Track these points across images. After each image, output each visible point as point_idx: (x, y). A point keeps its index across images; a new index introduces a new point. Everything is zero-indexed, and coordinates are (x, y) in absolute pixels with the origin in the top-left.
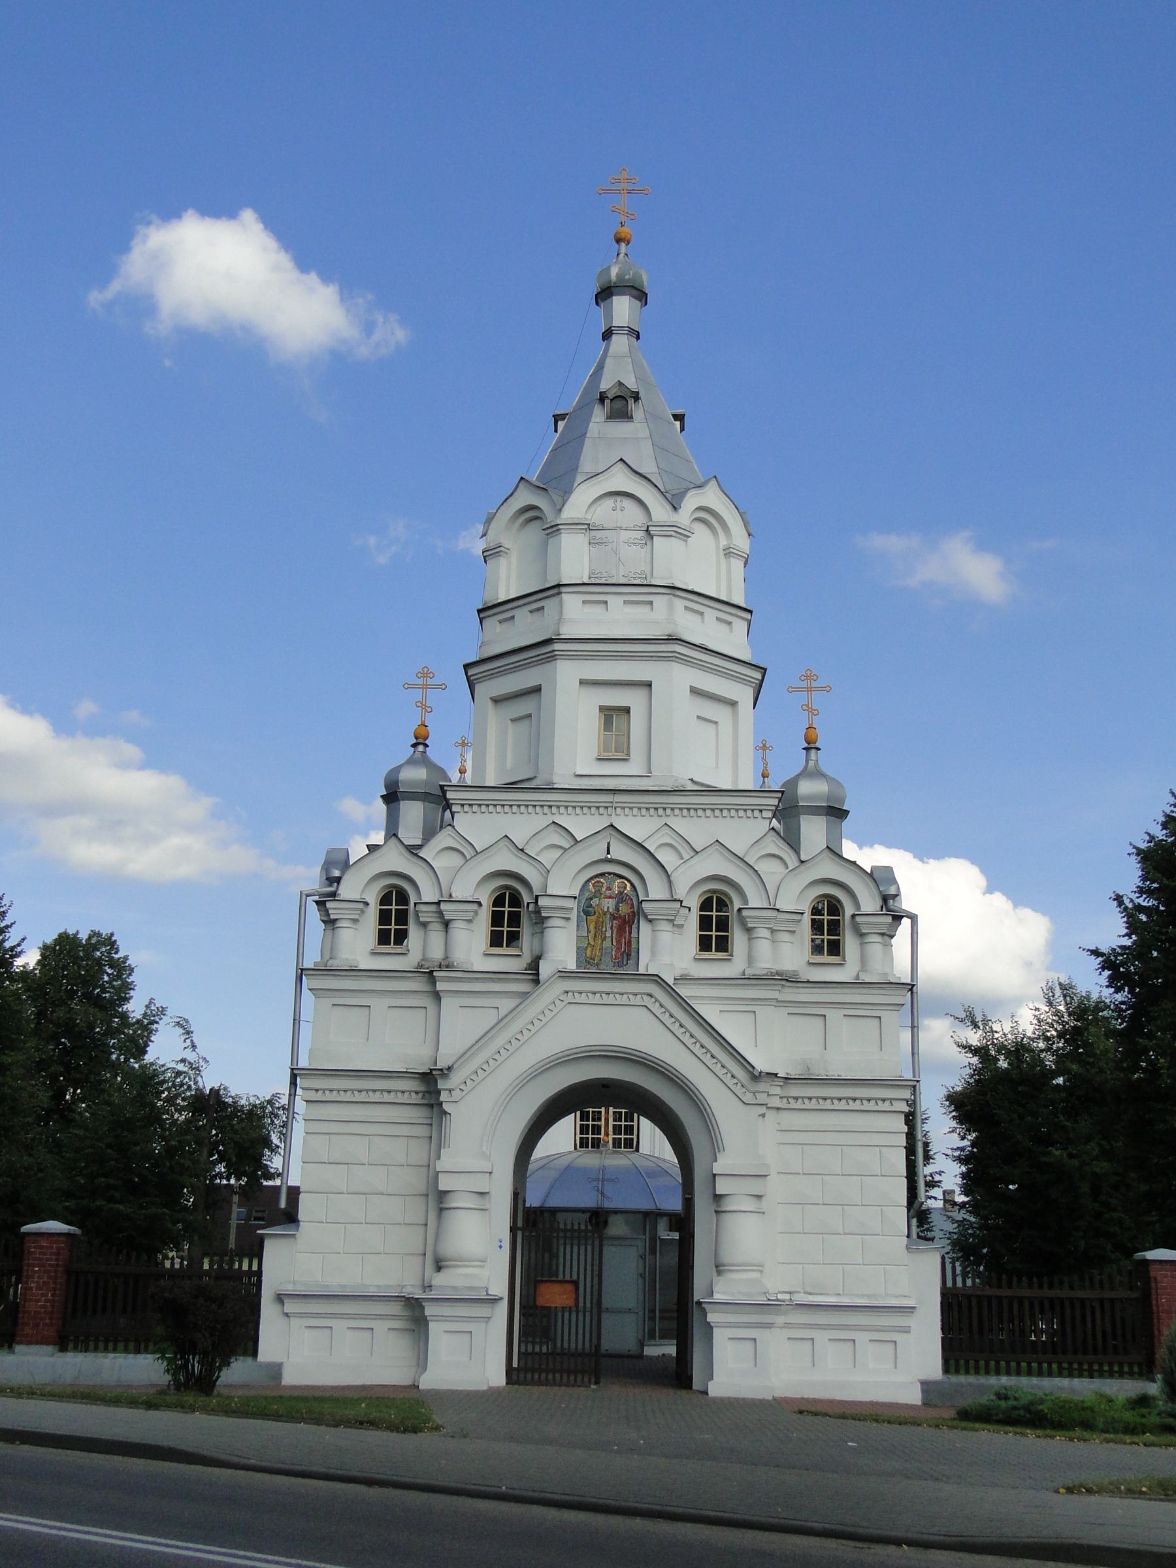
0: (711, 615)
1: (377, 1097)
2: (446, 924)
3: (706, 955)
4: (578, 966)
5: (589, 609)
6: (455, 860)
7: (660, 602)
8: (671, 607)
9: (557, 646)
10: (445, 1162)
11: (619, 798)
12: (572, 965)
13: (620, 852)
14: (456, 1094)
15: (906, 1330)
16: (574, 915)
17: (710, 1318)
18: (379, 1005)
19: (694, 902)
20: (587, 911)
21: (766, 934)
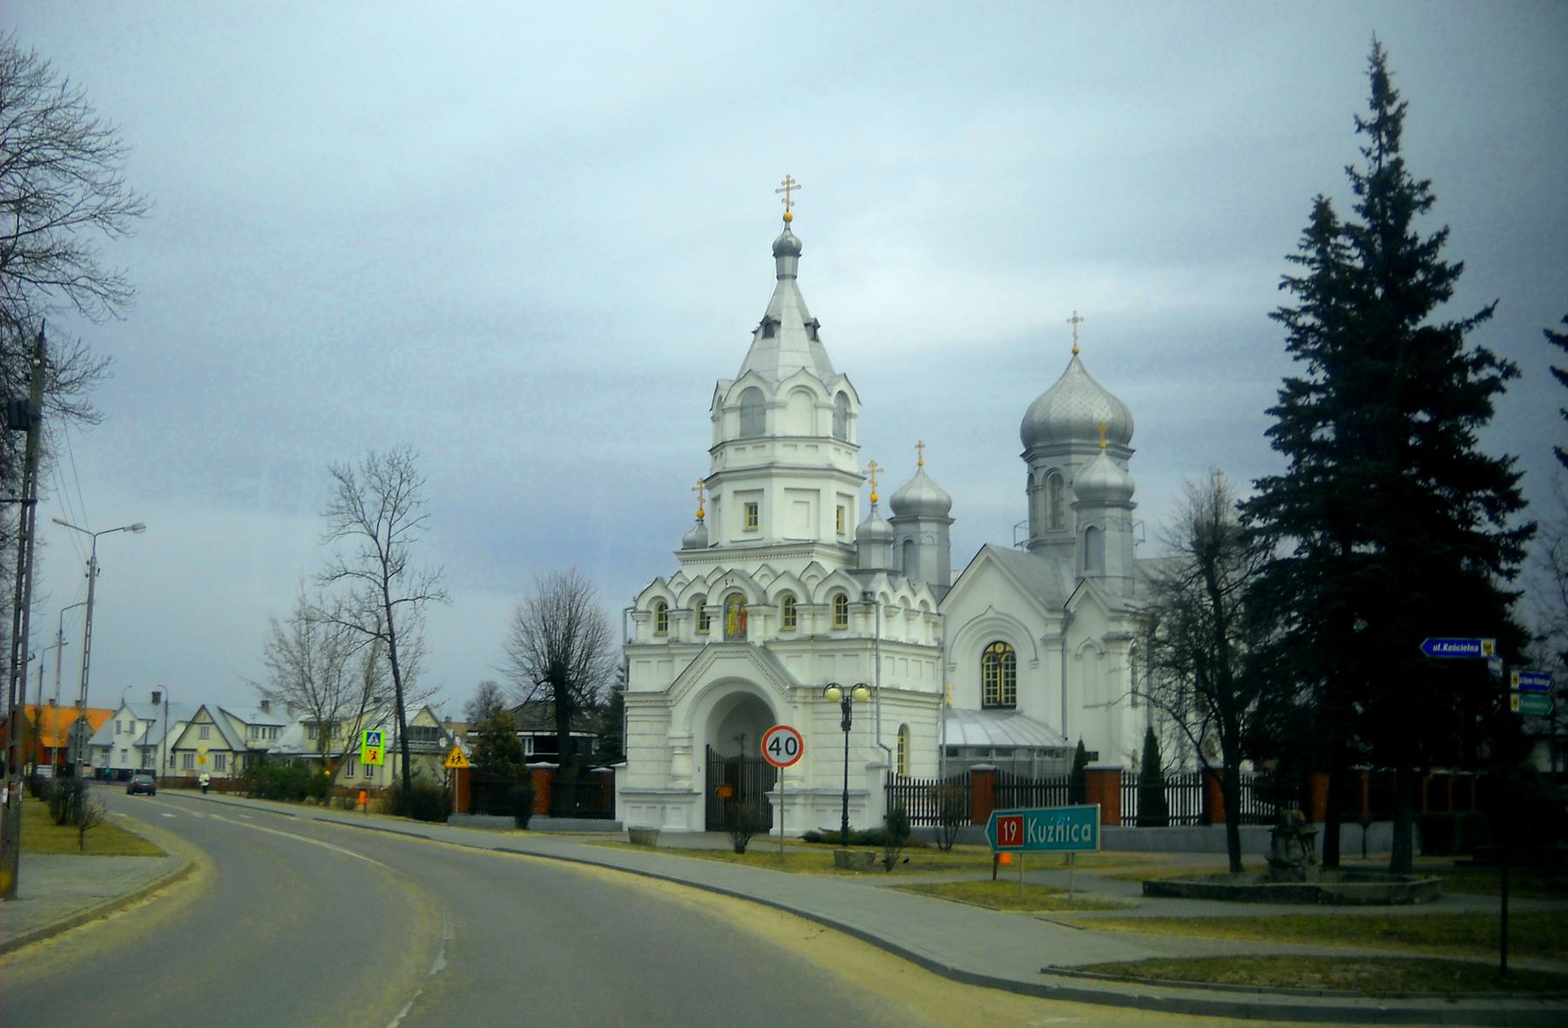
0: (801, 445)
1: (653, 704)
2: (678, 620)
3: (788, 628)
4: (725, 639)
5: (739, 452)
6: (680, 589)
7: (768, 445)
8: (773, 448)
9: (721, 476)
10: (671, 733)
11: (748, 552)
12: (720, 639)
13: (737, 583)
14: (674, 703)
15: (863, 806)
16: (721, 615)
17: (770, 801)
18: (654, 661)
19: (780, 603)
20: (727, 611)
21: (810, 617)
